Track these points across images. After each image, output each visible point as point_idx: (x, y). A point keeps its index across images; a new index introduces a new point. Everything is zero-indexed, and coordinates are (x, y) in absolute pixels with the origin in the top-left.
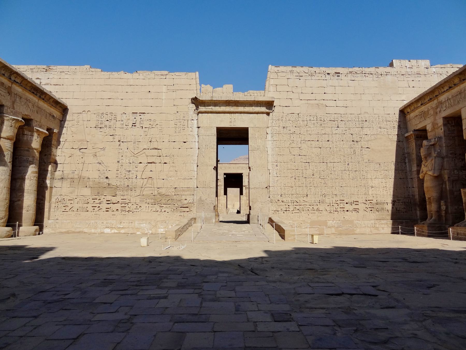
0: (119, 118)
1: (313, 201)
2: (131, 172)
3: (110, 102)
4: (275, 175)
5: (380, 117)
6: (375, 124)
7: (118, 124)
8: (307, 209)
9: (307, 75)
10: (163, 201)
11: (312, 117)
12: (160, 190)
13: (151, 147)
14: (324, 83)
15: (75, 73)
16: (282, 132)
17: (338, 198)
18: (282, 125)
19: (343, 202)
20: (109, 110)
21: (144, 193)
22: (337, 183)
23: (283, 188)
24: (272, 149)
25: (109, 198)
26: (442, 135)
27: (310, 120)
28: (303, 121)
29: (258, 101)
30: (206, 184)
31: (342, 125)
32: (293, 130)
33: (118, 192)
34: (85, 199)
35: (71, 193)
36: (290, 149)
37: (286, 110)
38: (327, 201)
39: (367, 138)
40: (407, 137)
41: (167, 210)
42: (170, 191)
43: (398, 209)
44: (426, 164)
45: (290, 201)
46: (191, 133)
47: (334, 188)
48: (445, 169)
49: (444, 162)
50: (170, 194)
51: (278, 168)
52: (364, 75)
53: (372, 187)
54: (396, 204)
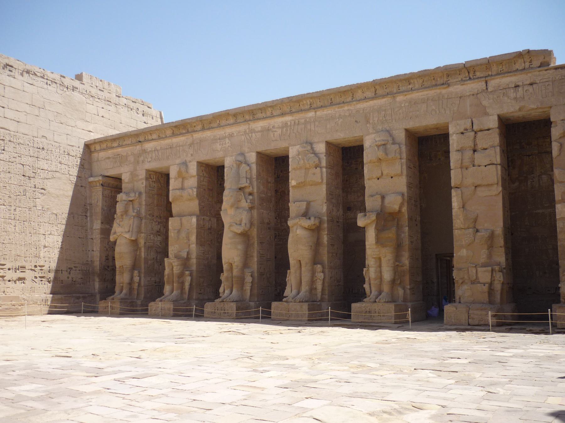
5: (61, 148)
26: (143, 190)
31: (10, 147)
39: (43, 174)
44: (121, 223)
48: (142, 233)
49: (141, 223)
52: (46, 81)
53: (45, 247)
54: (72, 272)
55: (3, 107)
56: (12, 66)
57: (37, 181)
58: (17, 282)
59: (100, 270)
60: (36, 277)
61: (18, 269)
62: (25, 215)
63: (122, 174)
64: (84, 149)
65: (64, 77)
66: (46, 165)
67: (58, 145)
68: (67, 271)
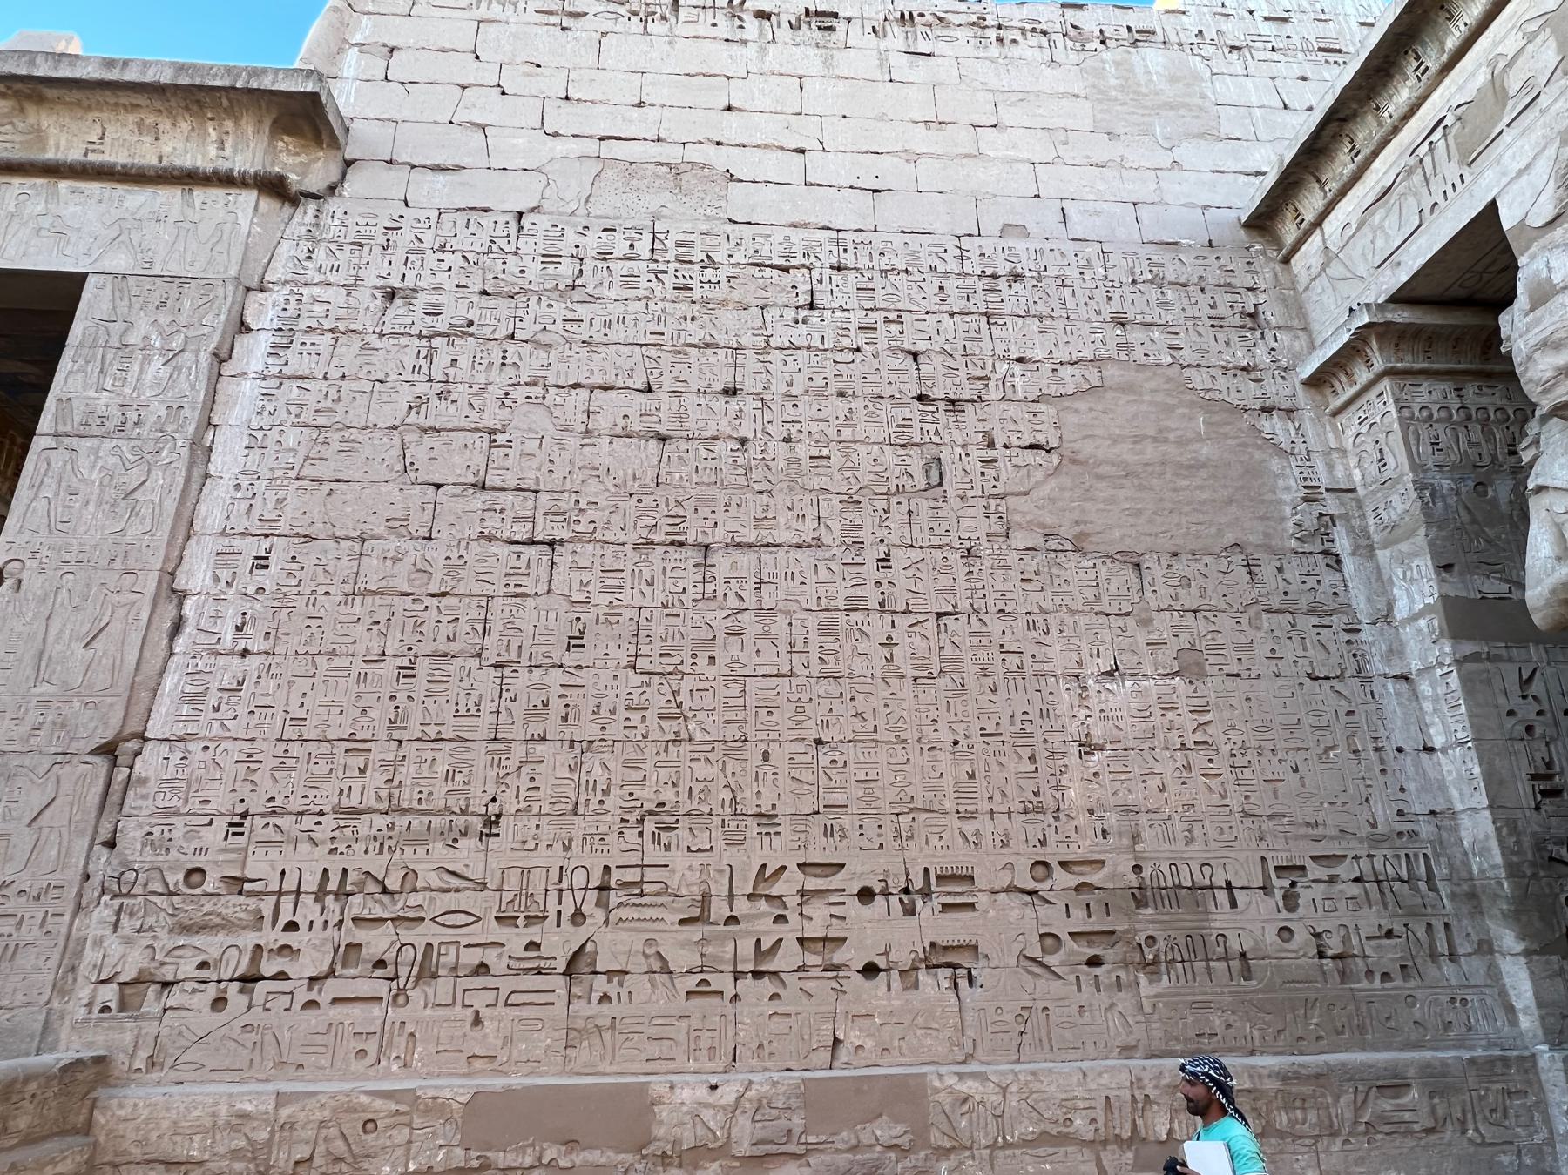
1: (538, 881)
4: (227, 643)
6: (1082, 297)
11: (618, 236)
14: (724, 59)
19: (836, 881)
22: (783, 719)
23: (268, 751)
27: (604, 256)
32: (454, 310)
37: (434, 192)
38: (683, 871)
39: (1022, 382)
43: (1334, 945)
45: (311, 883)
47: (753, 754)
51: (265, 579)
52: (992, 34)
53: (1088, 747)
54: (1304, 896)
55: (802, 151)
58: (923, 976)
59: (1513, 870)
60: (1050, 939)
62: (945, 581)
63: (1493, 205)
66: (1037, 338)
68: (1266, 888)
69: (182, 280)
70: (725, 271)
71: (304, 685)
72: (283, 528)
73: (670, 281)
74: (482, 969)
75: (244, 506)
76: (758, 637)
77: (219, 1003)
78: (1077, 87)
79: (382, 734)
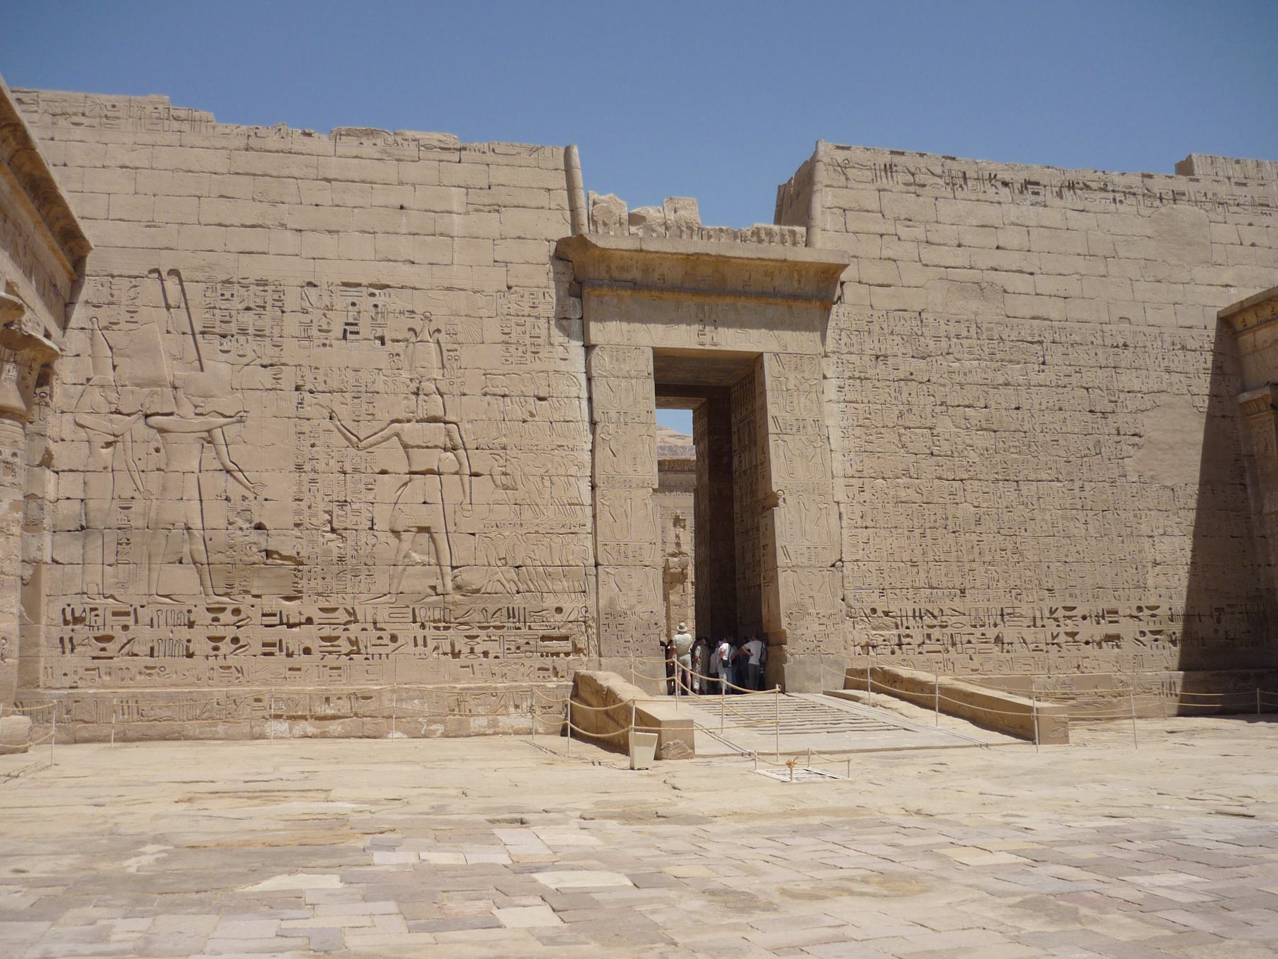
0: (291, 301)
1: (981, 613)
2: (348, 508)
3: (253, 240)
4: (859, 524)
5: (1166, 337)
7: (292, 324)
8: (965, 638)
9: (941, 182)
10: (477, 617)
12: (466, 576)
13: (421, 414)
15: (109, 119)
16: (870, 373)
17: (1057, 603)
18: (871, 346)
20: (253, 269)
21: (406, 585)
24: (844, 430)
25: (273, 603)
28: (937, 338)
29: (796, 263)
30: (630, 555)
31: (1055, 356)
33: (304, 582)
34: (177, 608)
35: (123, 585)
36: (902, 431)
37: (883, 299)
38: (1025, 609)
39: (1132, 403)
40: (1242, 405)
41: (493, 648)
42: (496, 578)
45: (910, 613)
46: (563, 366)
50: (499, 588)
52: (1111, 195)
53: (1156, 564)
55: (1032, 274)
56: (1037, 184)
57: (1121, 419)
58: (1104, 644)
60: (1143, 633)
61: (1103, 617)
64: (1219, 330)
65: (1150, 177)
66: (1135, 380)
67: (1157, 331)
68: (1211, 616)
69: (802, 356)
70: (1008, 344)
71: (890, 540)
72: (865, 474)
73: (985, 349)
74: (969, 642)
75: (848, 464)
76: (1043, 520)
77: (893, 653)
78: (1148, 232)
79: (920, 558)
